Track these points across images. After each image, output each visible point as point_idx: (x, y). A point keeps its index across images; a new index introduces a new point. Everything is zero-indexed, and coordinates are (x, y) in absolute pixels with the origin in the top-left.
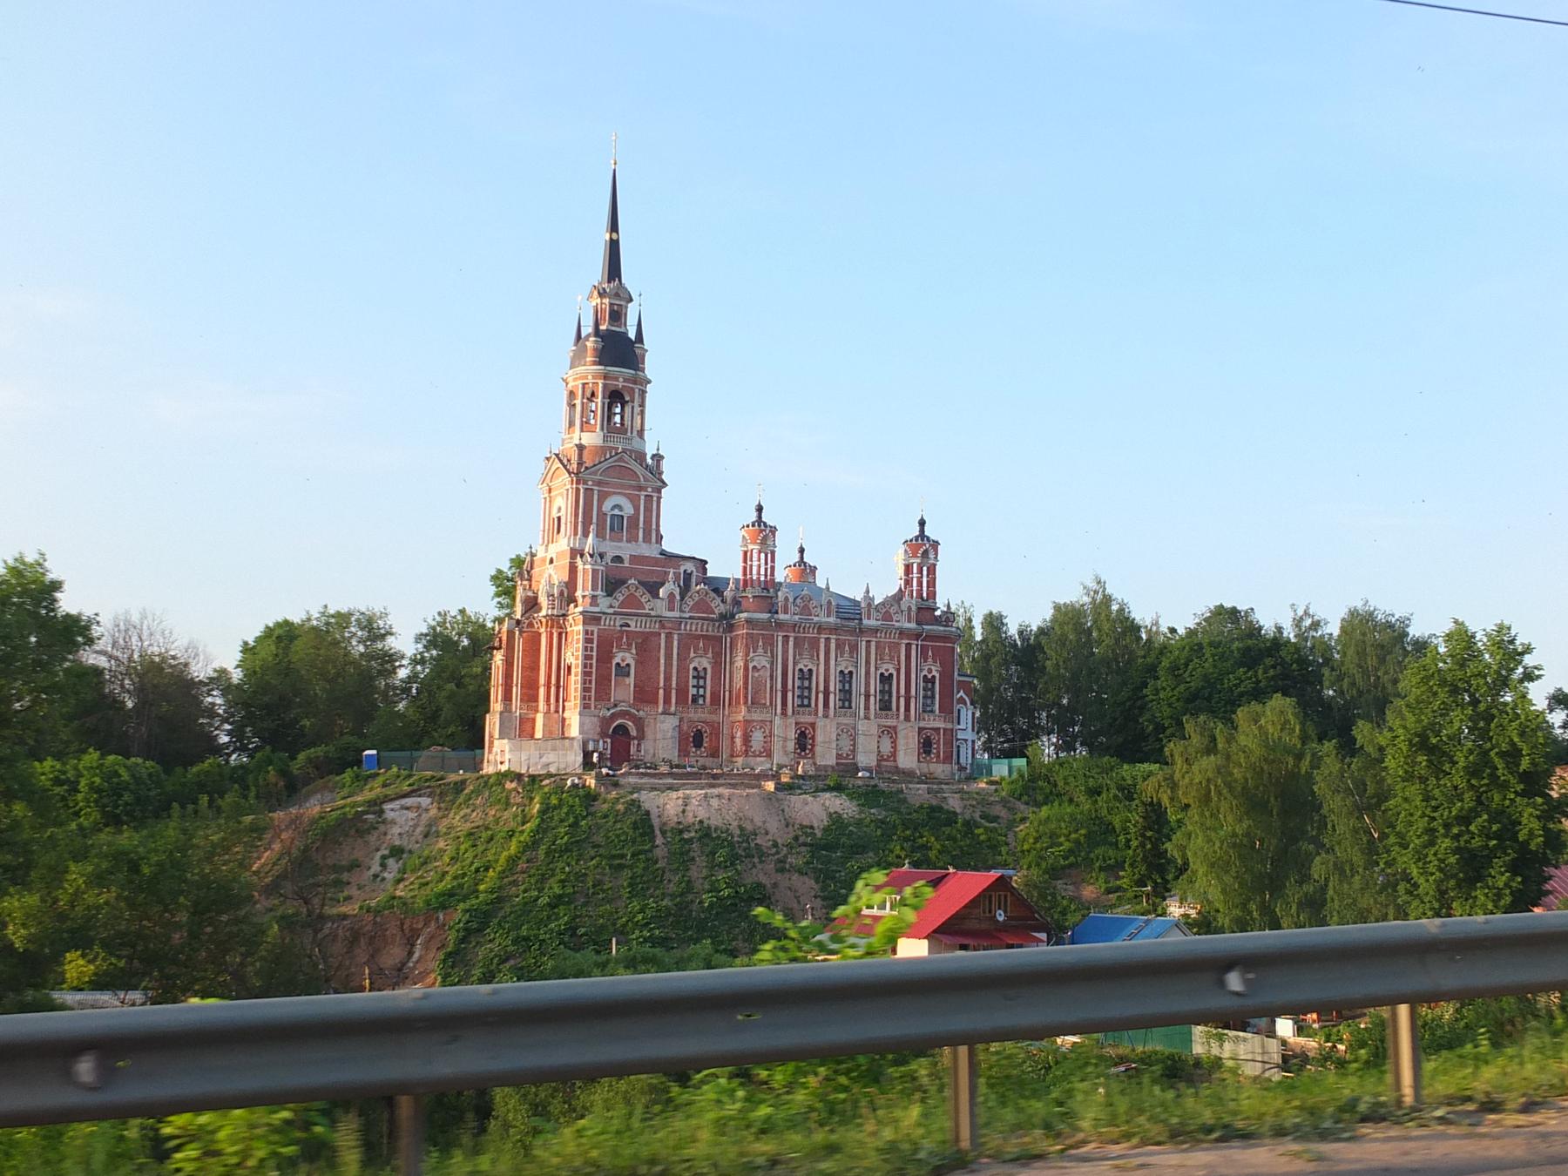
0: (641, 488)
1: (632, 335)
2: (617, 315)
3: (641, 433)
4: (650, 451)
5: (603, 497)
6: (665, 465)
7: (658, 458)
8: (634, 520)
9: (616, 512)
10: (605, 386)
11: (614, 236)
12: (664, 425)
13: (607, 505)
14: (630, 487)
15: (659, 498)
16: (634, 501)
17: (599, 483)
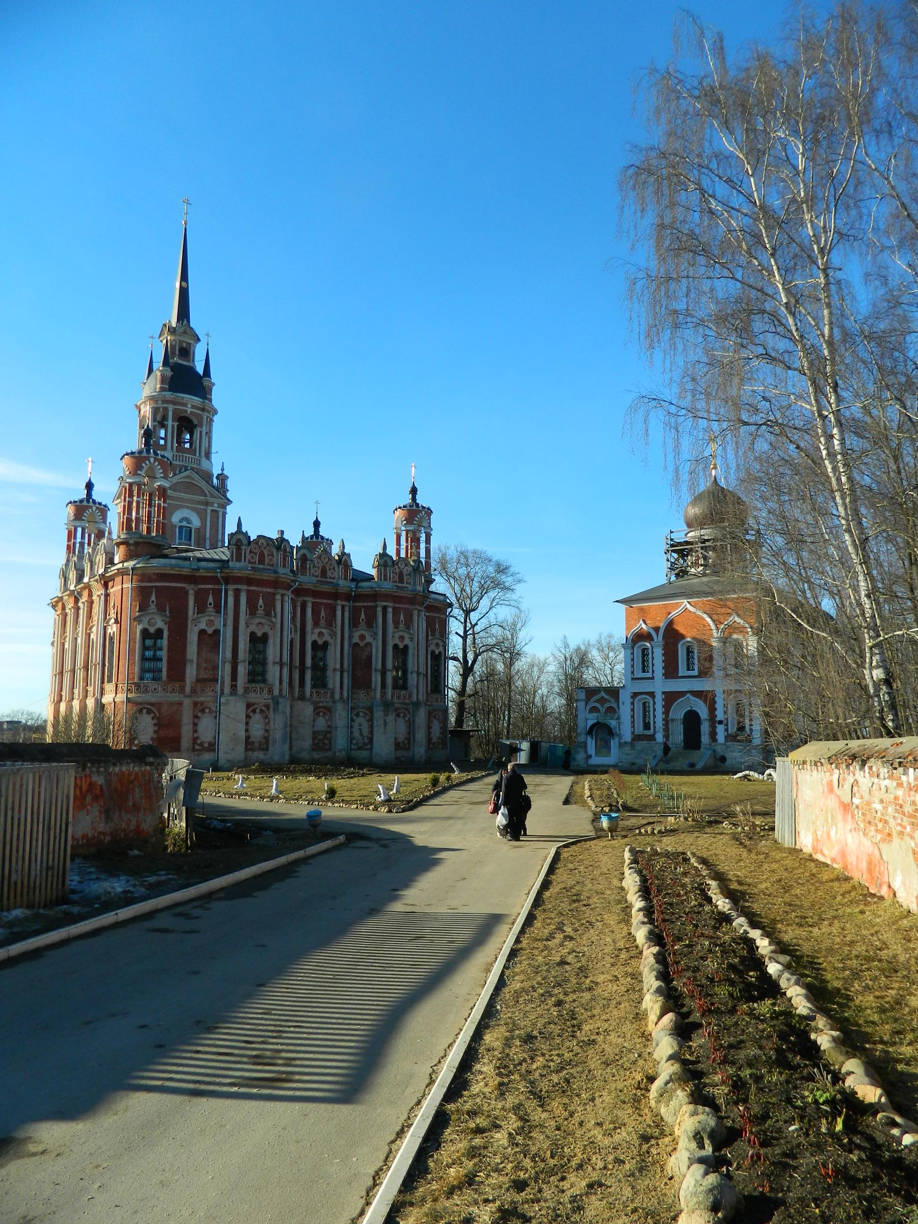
0: (207, 504)
1: (200, 369)
2: (186, 352)
3: (208, 455)
4: (216, 471)
6: (230, 484)
7: (222, 478)
8: (200, 531)
9: (184, 524)
10: (175, 412)
11: (184, 284)
12: (229, 447)
13: (176, 518)
14: (199, 502)
15: (224, 514)
16: (202, 516)
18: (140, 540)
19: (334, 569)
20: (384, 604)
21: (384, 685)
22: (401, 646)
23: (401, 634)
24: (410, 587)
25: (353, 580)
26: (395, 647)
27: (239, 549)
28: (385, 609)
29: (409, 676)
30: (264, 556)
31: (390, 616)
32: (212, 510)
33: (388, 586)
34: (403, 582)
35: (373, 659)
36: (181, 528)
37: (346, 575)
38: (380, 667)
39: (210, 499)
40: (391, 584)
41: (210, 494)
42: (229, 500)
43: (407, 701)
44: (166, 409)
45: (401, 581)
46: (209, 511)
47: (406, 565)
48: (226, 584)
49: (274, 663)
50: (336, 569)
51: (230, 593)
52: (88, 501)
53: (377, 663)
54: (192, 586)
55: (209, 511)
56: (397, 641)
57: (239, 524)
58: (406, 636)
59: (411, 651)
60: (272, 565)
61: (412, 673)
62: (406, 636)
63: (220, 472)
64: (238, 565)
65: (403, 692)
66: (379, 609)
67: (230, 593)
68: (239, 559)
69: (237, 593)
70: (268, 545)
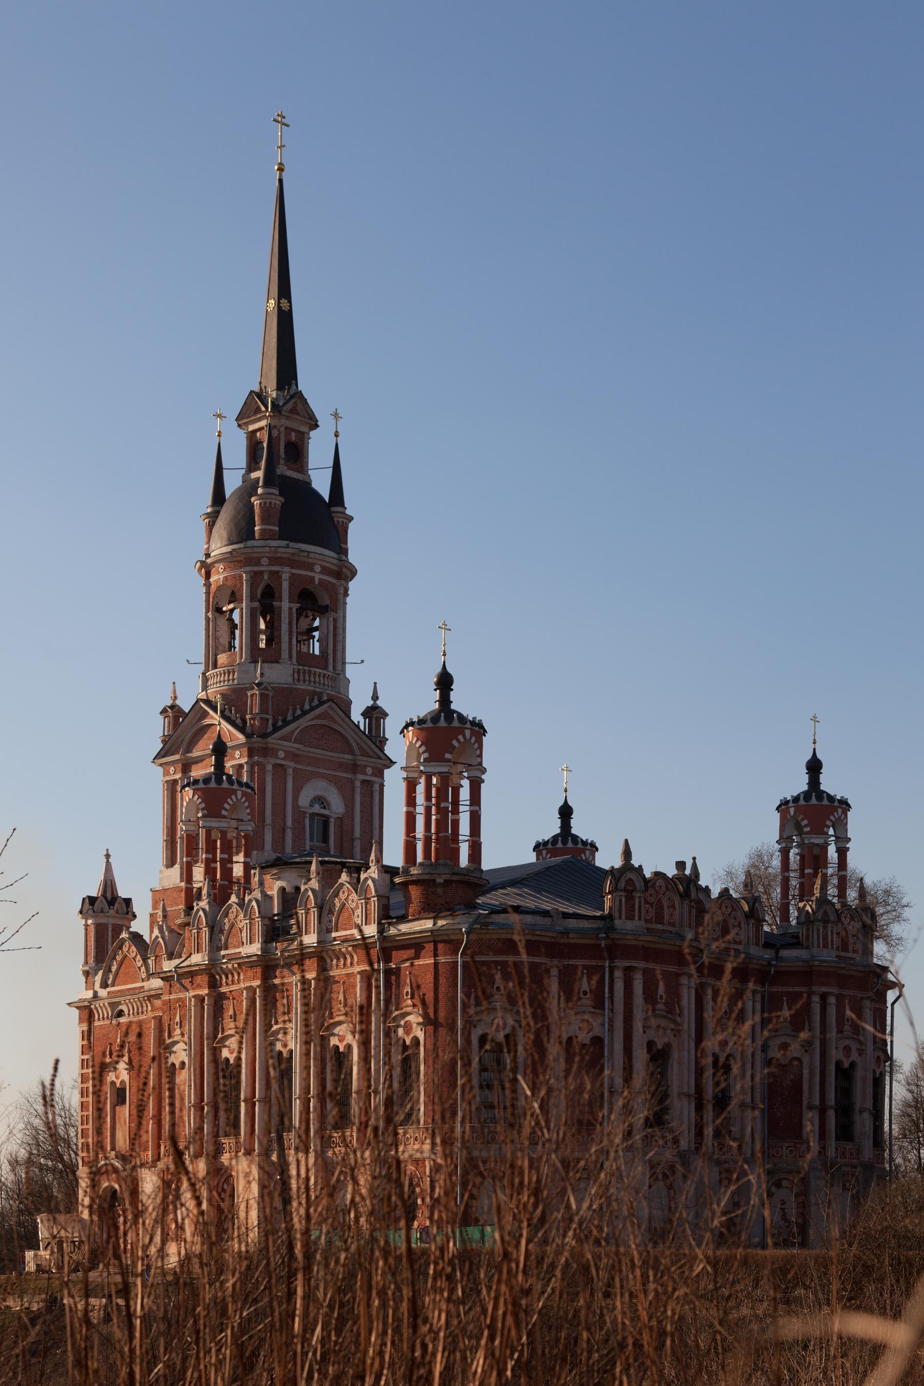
0: (354, 768)
1: (325, 494)
5: (301, 781)
9: (317, 809)
13: (304, 800)
14: (341, 766)
15: (382, 786)
17: (293, 756)
18: (455, 878)
19: (739, 926)
20: (824, 989)
21: (823, 1135)
22: (846, 1065)
23: (847, 1042)
24: (858, 958)
25: (767, 945)
26: (838, 1064)
27: (630, 898)
28: (824, 997)
29: (857, 1117)
30: (662, 908)
31: (832, 1011)
32: (363, 782)
33: (828, 956)
34: (846, 950)
35: (805, 1087)
36: (313, 815)
37: (757, 938)
38: (817, 1102)
39: (362, 760)
40: (834, 953)
41: (360, 748)
42: (391, 761)
43: (854, 1161)
44: (276, 575)
45: (844, 946)
46: (358, 784)
47: (852, 919)
48: (612, 958)
49: (680, 1095)
50: (743, 926)
51: (618, 974)
52: (219, 781)
53: (811, 1094)
54: (556, 962)
55: (358, 784)
56: (841, 1056)
57: (627, 853)
58: (854, 1046)
59: (859, 1074)
60: (673, 925)
61: (861, 1112)
62: (854, 1046)
63: (370, 703)
64: (630, 925)
65: (849, 1146)
66: (816, 999)
67: (618, 974)
68: (630, 917)
69: (628, 972)
70: (667, 889)
